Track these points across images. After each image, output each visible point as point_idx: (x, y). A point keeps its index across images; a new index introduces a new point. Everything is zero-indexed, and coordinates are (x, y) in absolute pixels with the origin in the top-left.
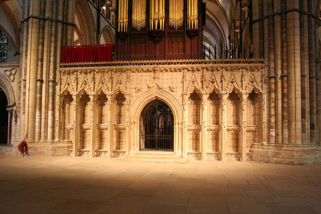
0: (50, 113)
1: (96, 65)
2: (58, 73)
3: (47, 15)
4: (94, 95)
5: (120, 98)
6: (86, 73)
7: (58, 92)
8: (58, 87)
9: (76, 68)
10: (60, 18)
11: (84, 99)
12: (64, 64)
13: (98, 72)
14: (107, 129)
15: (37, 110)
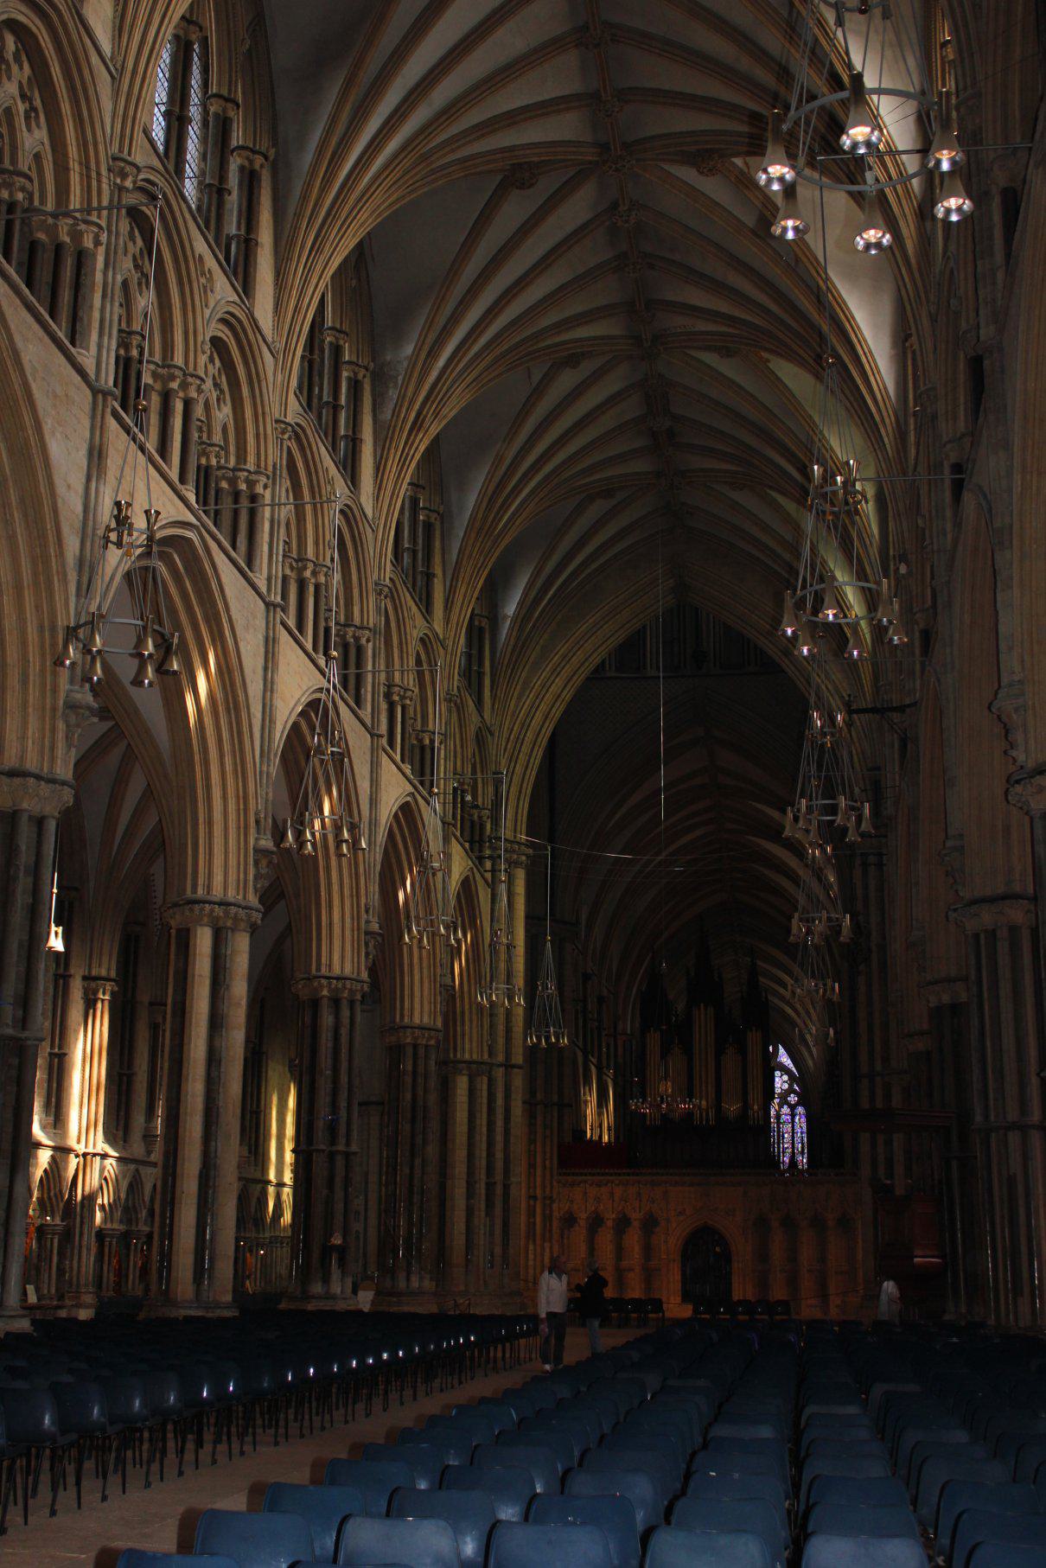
0: (547, 1245)
1: (616, 1174)
2: (555, 1184)
3: (539, 1096)
4: (613, 1220)
5: (650, 1224)
6: (600, 1186)
7: (556, 1214)
8: (555, 1206)
9: (584, 1177)
10: (555, 1098)
11: (596, 1222)
12: (564, 1171)
13: (618, 1185)
14: (631, 1270)
15: (531, 1242)
